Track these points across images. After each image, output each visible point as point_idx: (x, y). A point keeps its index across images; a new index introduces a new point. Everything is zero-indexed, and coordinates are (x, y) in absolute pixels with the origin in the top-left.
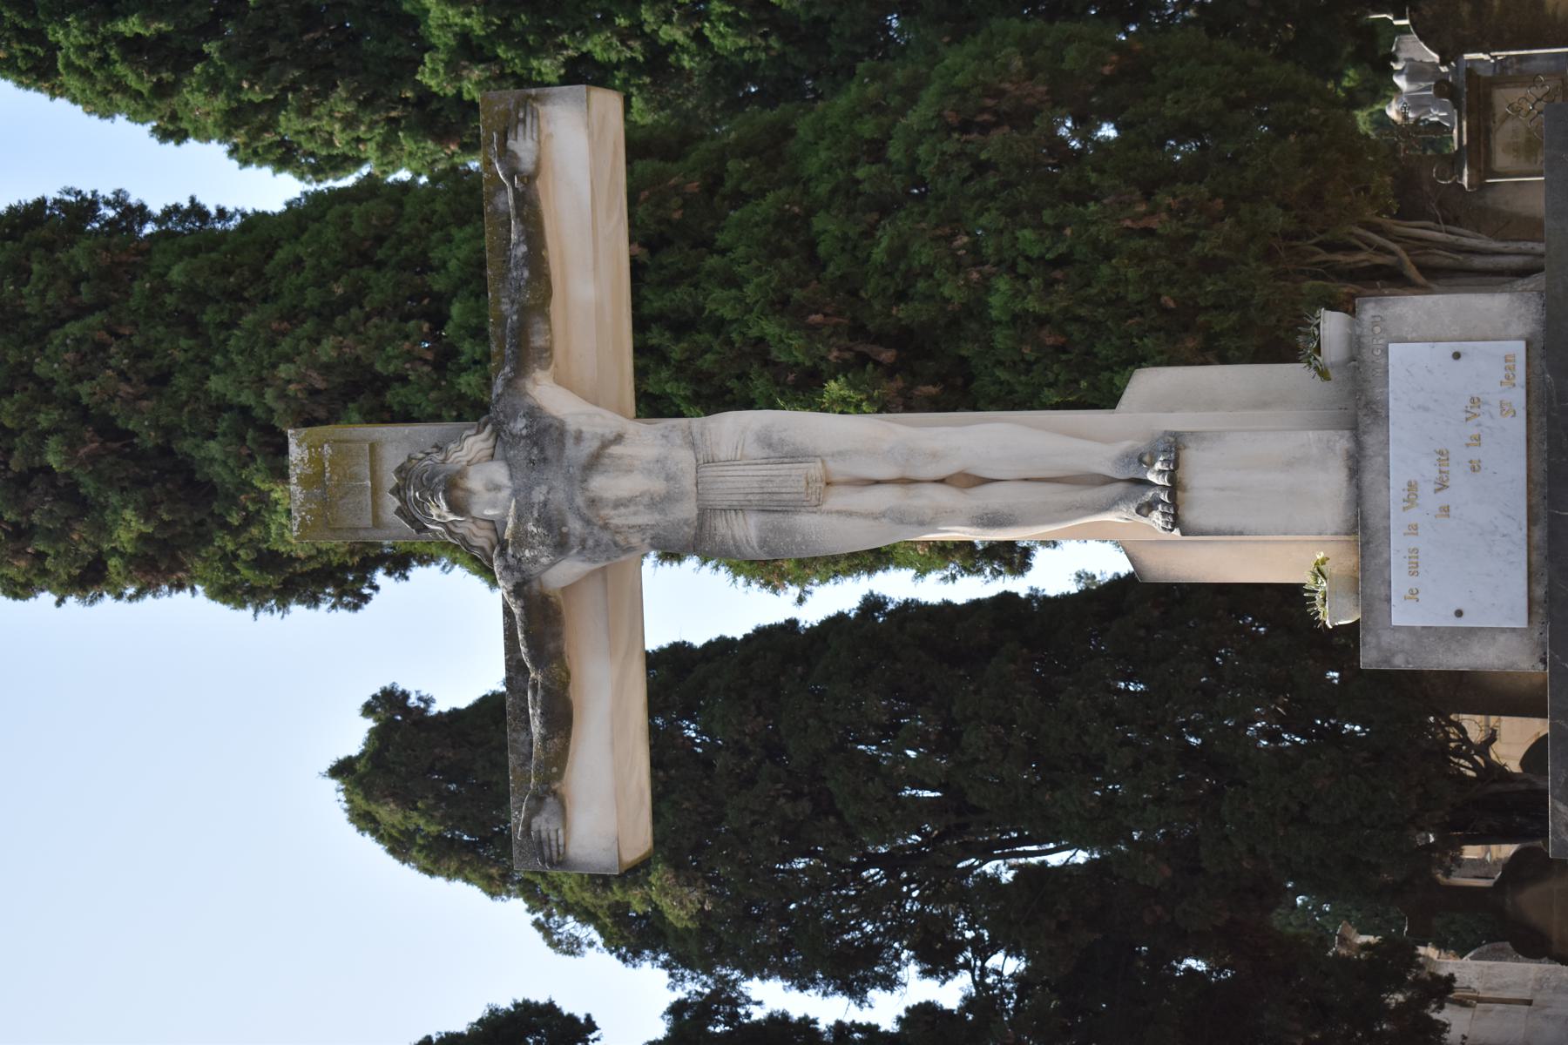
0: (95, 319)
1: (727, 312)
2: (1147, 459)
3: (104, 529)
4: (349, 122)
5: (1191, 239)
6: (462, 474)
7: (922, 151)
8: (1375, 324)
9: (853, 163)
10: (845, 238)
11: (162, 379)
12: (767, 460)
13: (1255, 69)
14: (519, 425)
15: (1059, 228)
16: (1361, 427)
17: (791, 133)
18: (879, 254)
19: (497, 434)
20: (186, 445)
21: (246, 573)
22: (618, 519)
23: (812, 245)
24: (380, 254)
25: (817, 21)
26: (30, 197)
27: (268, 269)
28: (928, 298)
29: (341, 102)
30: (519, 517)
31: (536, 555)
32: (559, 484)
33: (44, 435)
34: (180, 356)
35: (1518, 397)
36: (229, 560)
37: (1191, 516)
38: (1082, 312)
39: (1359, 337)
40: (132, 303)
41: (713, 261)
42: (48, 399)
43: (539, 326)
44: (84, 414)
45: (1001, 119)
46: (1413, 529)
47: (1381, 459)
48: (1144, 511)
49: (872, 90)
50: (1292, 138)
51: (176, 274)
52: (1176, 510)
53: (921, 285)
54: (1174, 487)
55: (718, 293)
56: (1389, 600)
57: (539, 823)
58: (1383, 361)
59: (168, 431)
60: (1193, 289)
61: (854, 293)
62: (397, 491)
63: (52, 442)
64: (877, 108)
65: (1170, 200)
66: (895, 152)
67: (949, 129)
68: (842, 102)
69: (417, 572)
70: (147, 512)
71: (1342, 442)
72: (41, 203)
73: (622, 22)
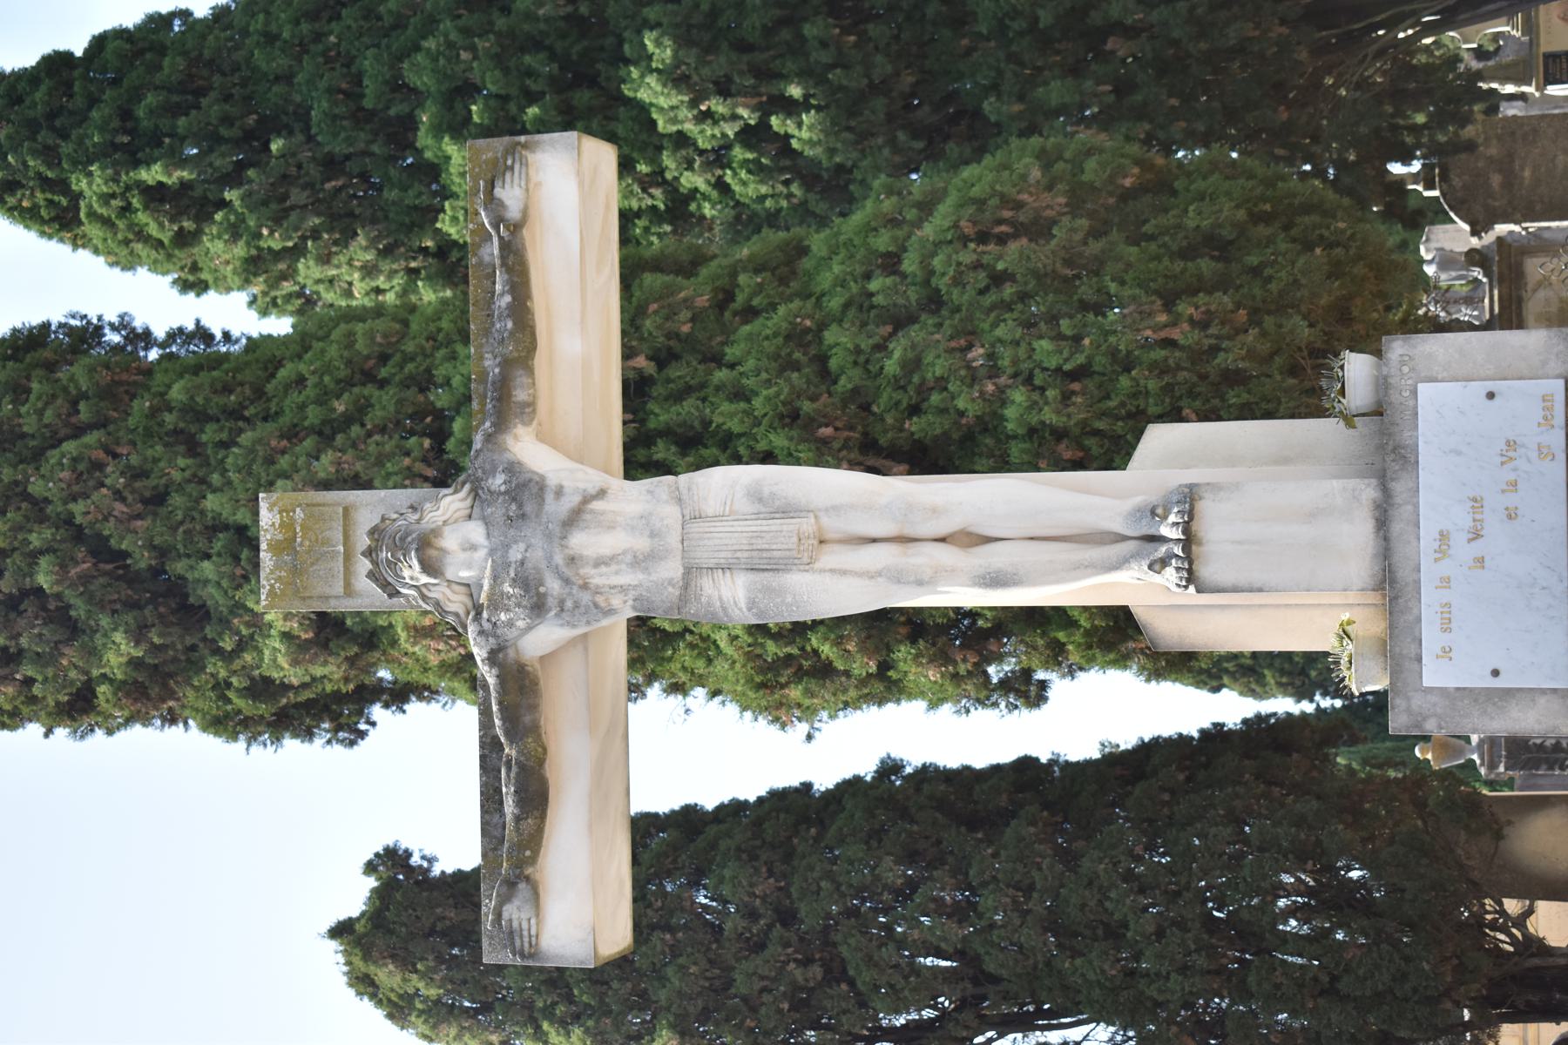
0: (91, 438)
1: (735, 426)
2: (1159, 511)
3: (93, 653)
4: (369, 271)
5: (1214, 350)
6: (436, 532)
7: (937, 262)
8: (1403, 363)
9: (868, 276)
10: (858, 351)
11: (158, 499)
12: (757, 516)
13: (1280, 184)
14: (498, 482)
15: (1077, 339)
16: (1389, 474)
17: (803, 251)
18: (891, 366)
19: (475, 494)
20: (179, 567)
21: (239, 702)
22: (598, 578)
23: (822, 359)
24: (384, 373)
25: (840, 168)
26: (36, 320)
27: (269, 388)
28: (943, 411)
29: (361, 250)
30: (495, 578)
31: (513, 618)
32: (538, 541)
33: (34, 556)
34: (177, 476)
36: (221, 687)
37: (1206, 571)
38: (1100, 425)
39: (1385, 378)
40: (131, 422)
41: (721, 375)
42: (42, 519)
43: (521, 378)
44: (78, 534)
45: (1019, 230)
46: (1446, 582)
47: (1410, 507)
48: (1157, 567)
49: (888, 204)
50: (1318, 251)
51: (177, 393)
52: (1191, 564)
53: (935, 398)
54: (1189, 541)
55: (726, 407)
56: (1419, 659)
57: (512, 911)
58: (1411, 403)
59: (163, 552)
60: (1216, 402)
61: (866, 408)
62: (369, 553)
63: (44, 562)
64: (893, 222)
65: (1191, 310)
66: (909, 265)
67: (965, 240)
68: (857, 218)
69: (414, 707)
70: (138, 634)
71: (1368, 491)
72: (45, 326)
73: (643, 168)
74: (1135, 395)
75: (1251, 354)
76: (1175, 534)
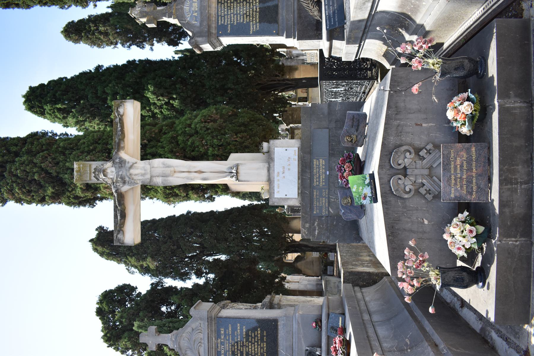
0: (45, 152)
1: (162, 153)
3: (45, 191)
4: (98, 124)
5: (244, 142)
6: (106, 169)
7: (197, 126)
9: (186, 128)
10: (183, 140)
11: (58, 163)
12: (164, 167)
14: (117, 160)
15: (221, 140)
17: (175, 123)
18: (189, 143)
19: (113, 162)
20: (61, 176)
21: (72, 200)
22: (135, 178)
23: (177, 142)
24: (99, 142)
25: (182, 110)
26: (36, 131)
27: (78, 144)
28: (198, 151)
29: (97, 121)
30: (117, 177)
31: (120, 184)
32: (124, 171)
33: (34, 173)
34: (61, 159)
35: (297, 157)
36: (69, 197)
37: (240, 178)
38: (224, 154)
40: (53, 149)
41: (160, 144)
42: (36, 166)
43: (122, 142)
44: (42, 169)
45: (211, 121)
46: (279, 180)
49: (189, 116)
51: (61, 144)
53: (197, 149)
54: (237, 173)
55: (160, 149)
57: (119, 236)
59: (58, 173)
61: (185, 150)
62: (94, 173)
63: (36, 174)
64: (190, 119)
66: (193, 126)
67: (202, 122)
68: (184, 118)
69: (104, 201)
70: (53, 188)
71: (266, 165)
72: (37, 132)
73: (148, 108)
74: (230, 149)
75: (250, 143)
76: (235, 172)
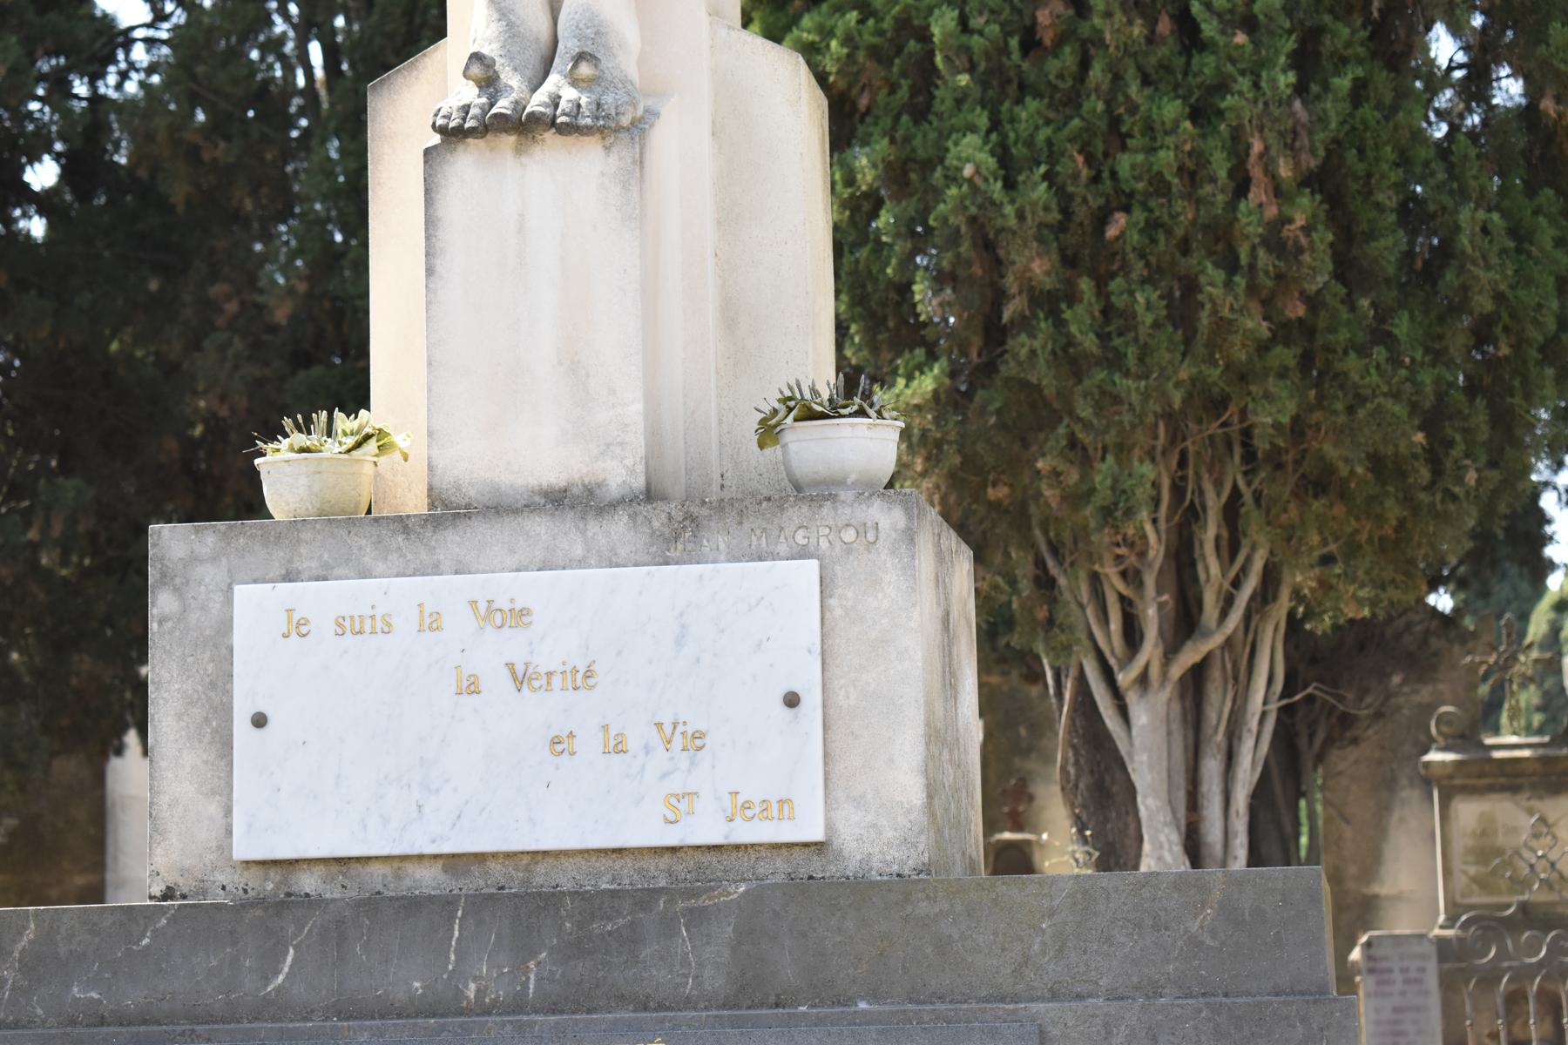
2: (585, 69)
5: (1231, 264)
8: (861, 530)
13: (1550, 372)
16: (644, 509)
35: (706, 829)
37: (466, 163)
38: (1097, 73)
39: (832, 498)
46: (432, 623)
47: (579, 551)
48: (476, 70)
50: (1419, 437)
52: (472, 132)
54: (524, 126)
56: (289, 577)
58: (782, 548)
60: (1139, 268)
65: (1300, 220)
74: (1149, 129)
75: (1223, 326)
76: (537, 102)
